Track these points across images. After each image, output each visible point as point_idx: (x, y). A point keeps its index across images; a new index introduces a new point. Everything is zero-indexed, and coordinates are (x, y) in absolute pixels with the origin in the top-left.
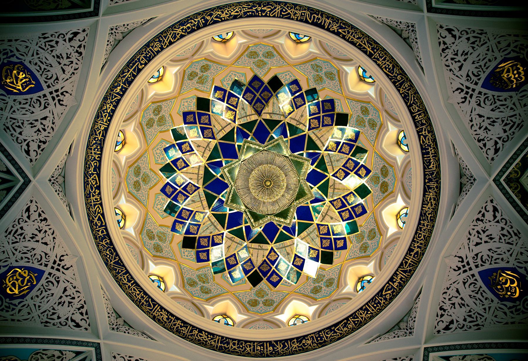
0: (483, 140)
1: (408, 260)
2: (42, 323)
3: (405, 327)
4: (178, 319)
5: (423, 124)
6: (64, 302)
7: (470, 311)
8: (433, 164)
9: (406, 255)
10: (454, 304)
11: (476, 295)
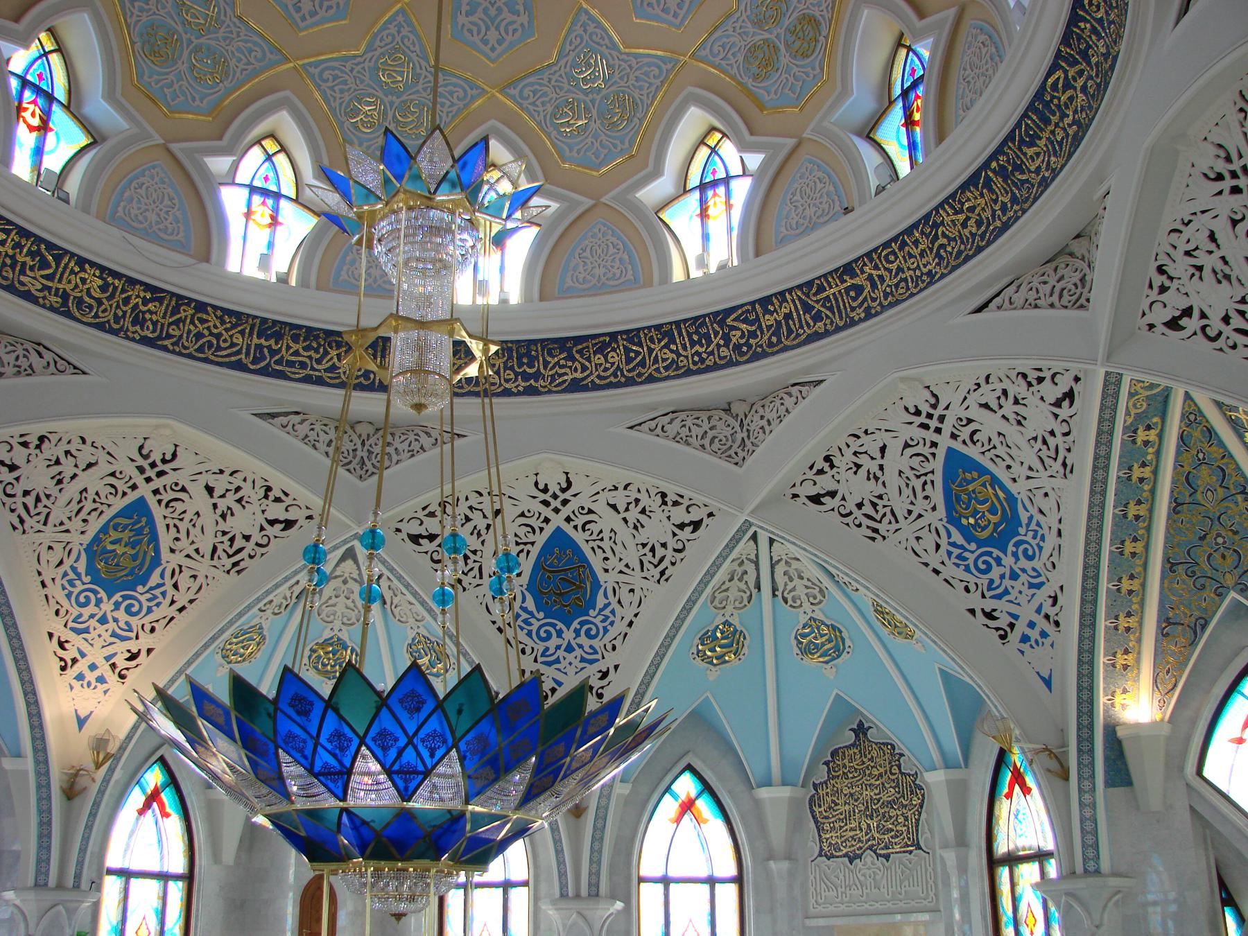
0: (1171, 278)
1: (831, 287)
3: (741, 416)
4: (132, 282)
5: (1085, 56)
7: (880, 497)
8: (1038, 154)
9: (830, 273)
10: (858, 466)
11: (913, 478)
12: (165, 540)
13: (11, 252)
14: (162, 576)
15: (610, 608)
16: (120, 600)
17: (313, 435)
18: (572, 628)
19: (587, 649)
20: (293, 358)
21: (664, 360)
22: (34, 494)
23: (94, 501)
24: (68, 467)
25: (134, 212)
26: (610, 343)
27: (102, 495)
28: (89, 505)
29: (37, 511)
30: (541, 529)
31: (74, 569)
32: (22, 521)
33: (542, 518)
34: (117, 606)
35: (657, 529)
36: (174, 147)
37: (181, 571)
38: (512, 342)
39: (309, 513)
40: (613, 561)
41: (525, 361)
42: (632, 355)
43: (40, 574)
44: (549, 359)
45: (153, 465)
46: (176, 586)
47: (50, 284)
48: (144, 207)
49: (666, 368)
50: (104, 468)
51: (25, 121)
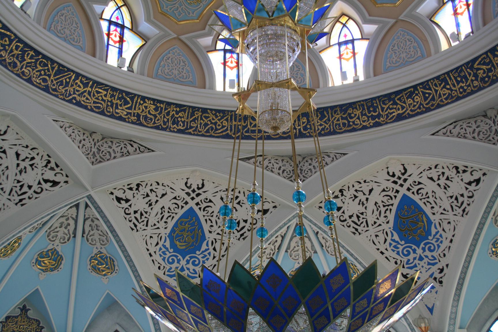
2: (16, 204)
3: (493, 117)
4: (169, 104)
6: (25, 168)
12: (206, 227)
13: (110, 99)
14: (207, 245)
15: (439, 234)
16: (189, 259)
17: (270, 166)
18: (421, 247)
19: (430, 258)
20: (254, 129)
21: (444, 95)
22: (139, 212)
23: (169, 212)
24: (153, 197)
25: (166, 71)
26: (414, 92)
27: (172, 209)
28: (166, 215)
29: (142, 220)
30: (395, 197)
31: (164, 246)
32: (136, 226)
33: (394, 191)
34: (188, 262)
35: (457, 187)
36: (183, 37)
37: (216, 242)
38: (363, 101)
39: (274, 205)
40: (436, 209)
41: (371, 109)
42: (427, 95)
43: (148, 250)
44: (384, 106)
45: (194, 191)
46: (214, 249)
47: (130, 111)
48: (171, 68)
49: (446, 99)
50: (170, 196)
51: (112, 40)
